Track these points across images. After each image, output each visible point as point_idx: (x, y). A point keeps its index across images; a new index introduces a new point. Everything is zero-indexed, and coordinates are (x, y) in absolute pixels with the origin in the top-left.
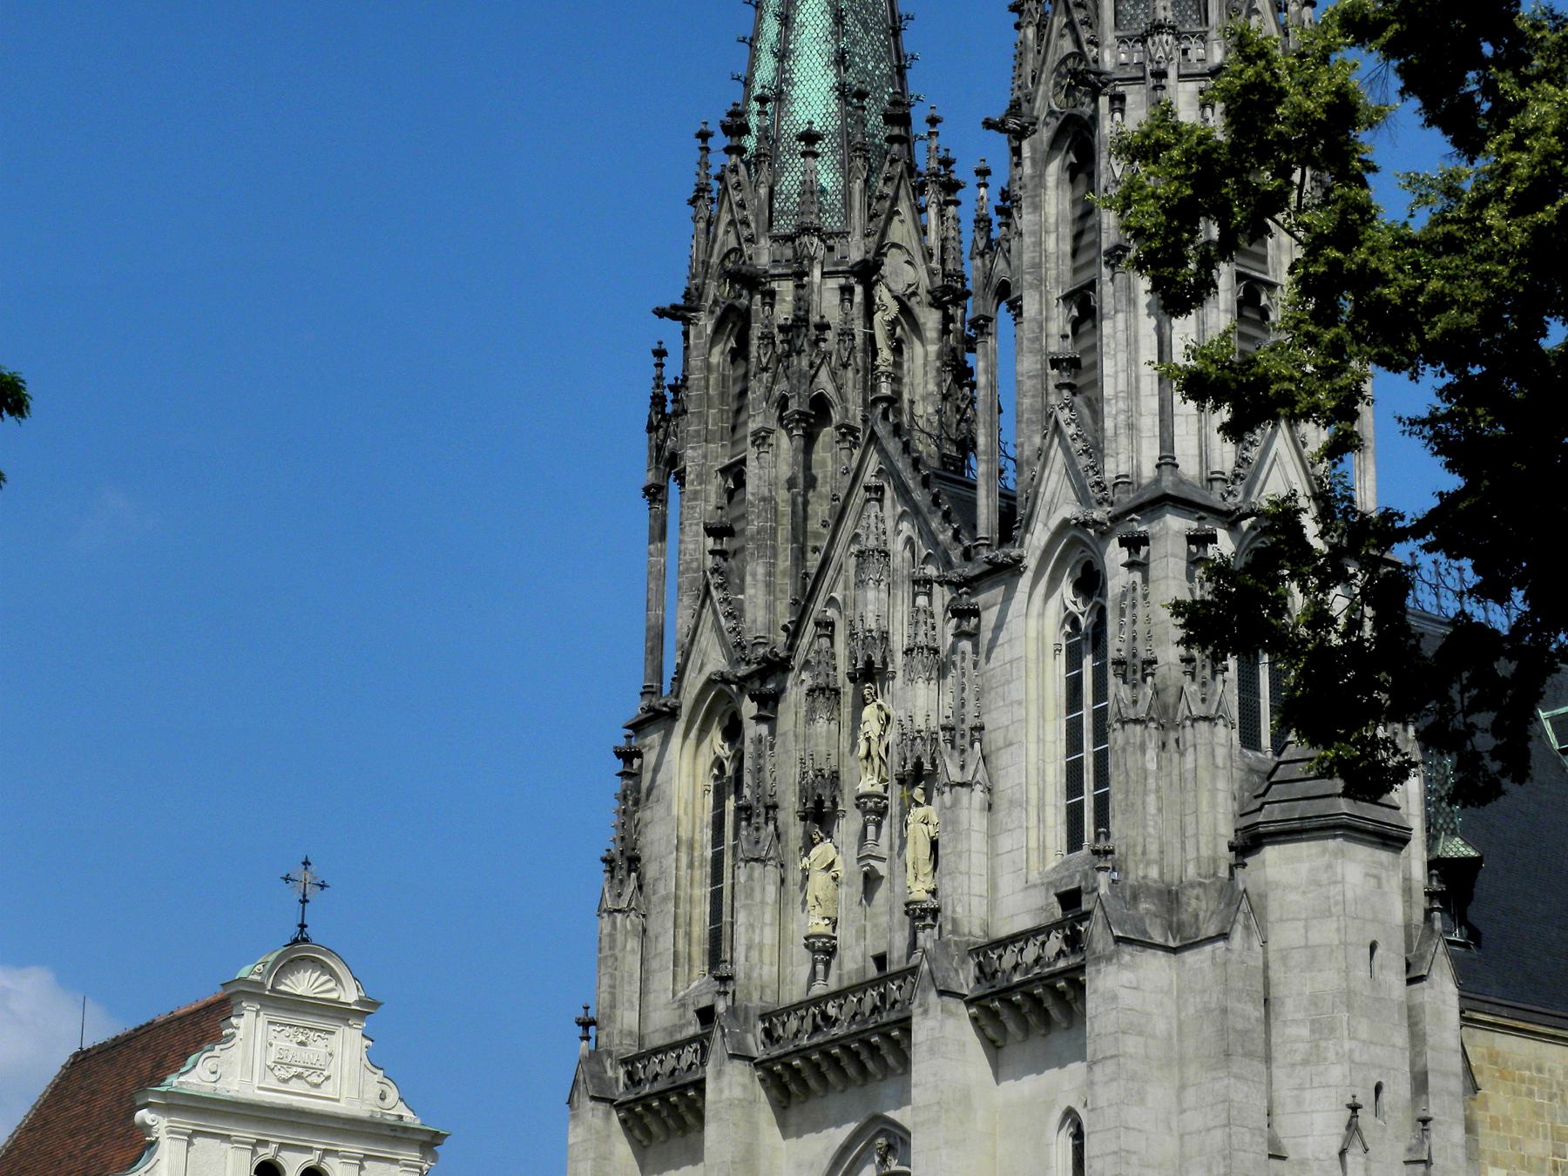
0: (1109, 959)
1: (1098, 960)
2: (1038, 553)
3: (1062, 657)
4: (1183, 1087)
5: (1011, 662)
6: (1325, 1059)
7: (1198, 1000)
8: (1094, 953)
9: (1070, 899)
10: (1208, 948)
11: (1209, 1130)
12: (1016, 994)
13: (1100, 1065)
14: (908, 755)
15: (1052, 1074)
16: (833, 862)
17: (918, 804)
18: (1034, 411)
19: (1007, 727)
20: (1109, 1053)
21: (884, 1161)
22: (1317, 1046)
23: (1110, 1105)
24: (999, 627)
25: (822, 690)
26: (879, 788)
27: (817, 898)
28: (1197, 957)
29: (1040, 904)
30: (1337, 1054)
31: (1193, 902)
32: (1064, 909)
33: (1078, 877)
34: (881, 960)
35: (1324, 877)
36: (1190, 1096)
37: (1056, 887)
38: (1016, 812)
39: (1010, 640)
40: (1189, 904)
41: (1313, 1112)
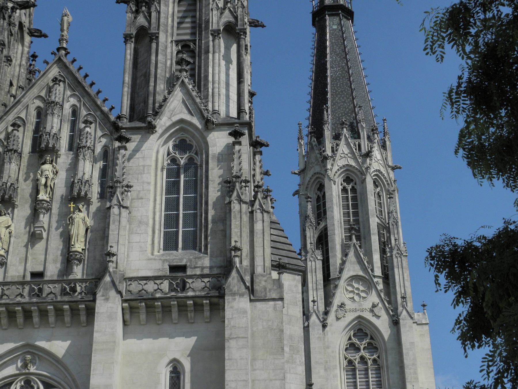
0: (242, 295)
1: (234, 294)
2: (164, 128)
3: (165, 172)
4: (254, 359)
5: (144, 166)
6: (295, 362)
7: (265, 324)
8: (231, 291)
9: (173, 269)
10: (272, 303)
11: (271, 380)
12: (158, 302)
13: (235, 340)
14: (83, 188)
15: (163, 341)
16: (10, 226)
17: (80, 211)
18: (162, 76)
19: (139, 191)
20: (241, 336)
21: (25, 366)
22: (292, 356)
23: (241, 359)
24: (136, 150)
25: (16, 151)
26: (48, 200)
28: (264, 306)
29: (158, 268)
30: (300, 361)
31: (263, 283)
32: (170, 272)
33: (185, 261)
34: (37, 275)
35: (294, 289)
36: (259, 364)
37: (169, 262)
39: (144, 157)
40: (260, 283)
41: (290, 383)
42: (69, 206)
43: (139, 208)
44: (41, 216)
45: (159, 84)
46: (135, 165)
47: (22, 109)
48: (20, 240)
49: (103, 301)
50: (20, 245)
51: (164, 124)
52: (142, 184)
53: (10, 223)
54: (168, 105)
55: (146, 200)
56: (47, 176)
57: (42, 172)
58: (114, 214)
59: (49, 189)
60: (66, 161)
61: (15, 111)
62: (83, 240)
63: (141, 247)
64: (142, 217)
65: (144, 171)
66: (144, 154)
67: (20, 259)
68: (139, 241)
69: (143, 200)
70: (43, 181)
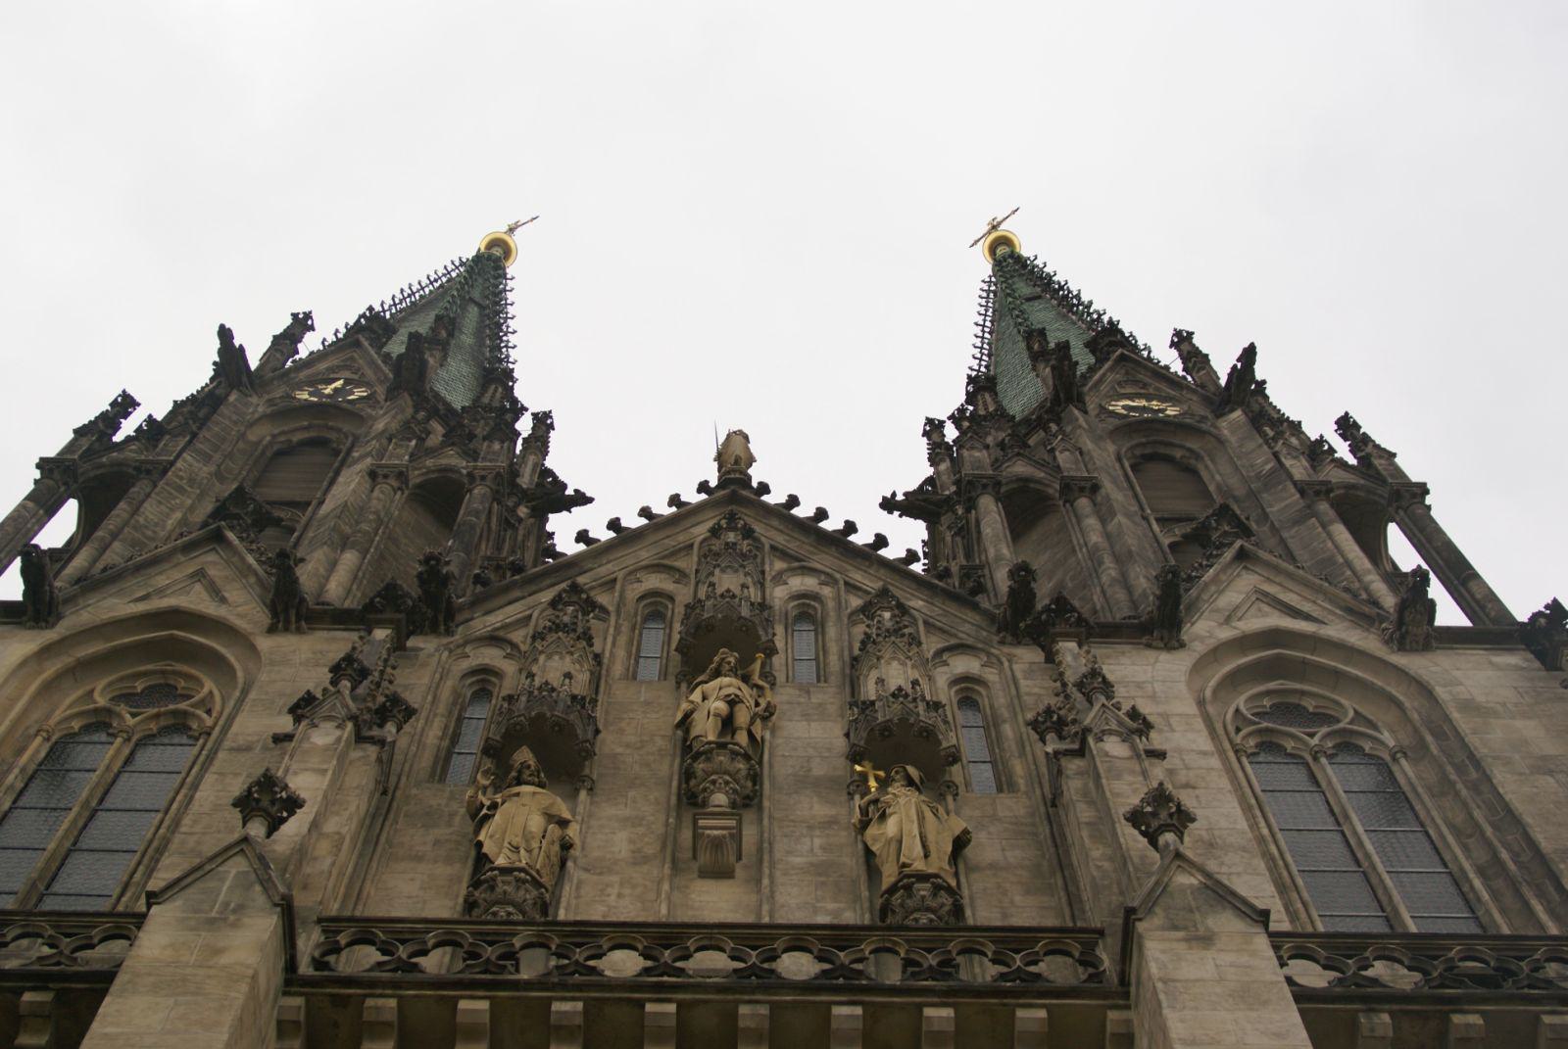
49: (1183, 946)
50: (614, 891)
69: (1197, 792)
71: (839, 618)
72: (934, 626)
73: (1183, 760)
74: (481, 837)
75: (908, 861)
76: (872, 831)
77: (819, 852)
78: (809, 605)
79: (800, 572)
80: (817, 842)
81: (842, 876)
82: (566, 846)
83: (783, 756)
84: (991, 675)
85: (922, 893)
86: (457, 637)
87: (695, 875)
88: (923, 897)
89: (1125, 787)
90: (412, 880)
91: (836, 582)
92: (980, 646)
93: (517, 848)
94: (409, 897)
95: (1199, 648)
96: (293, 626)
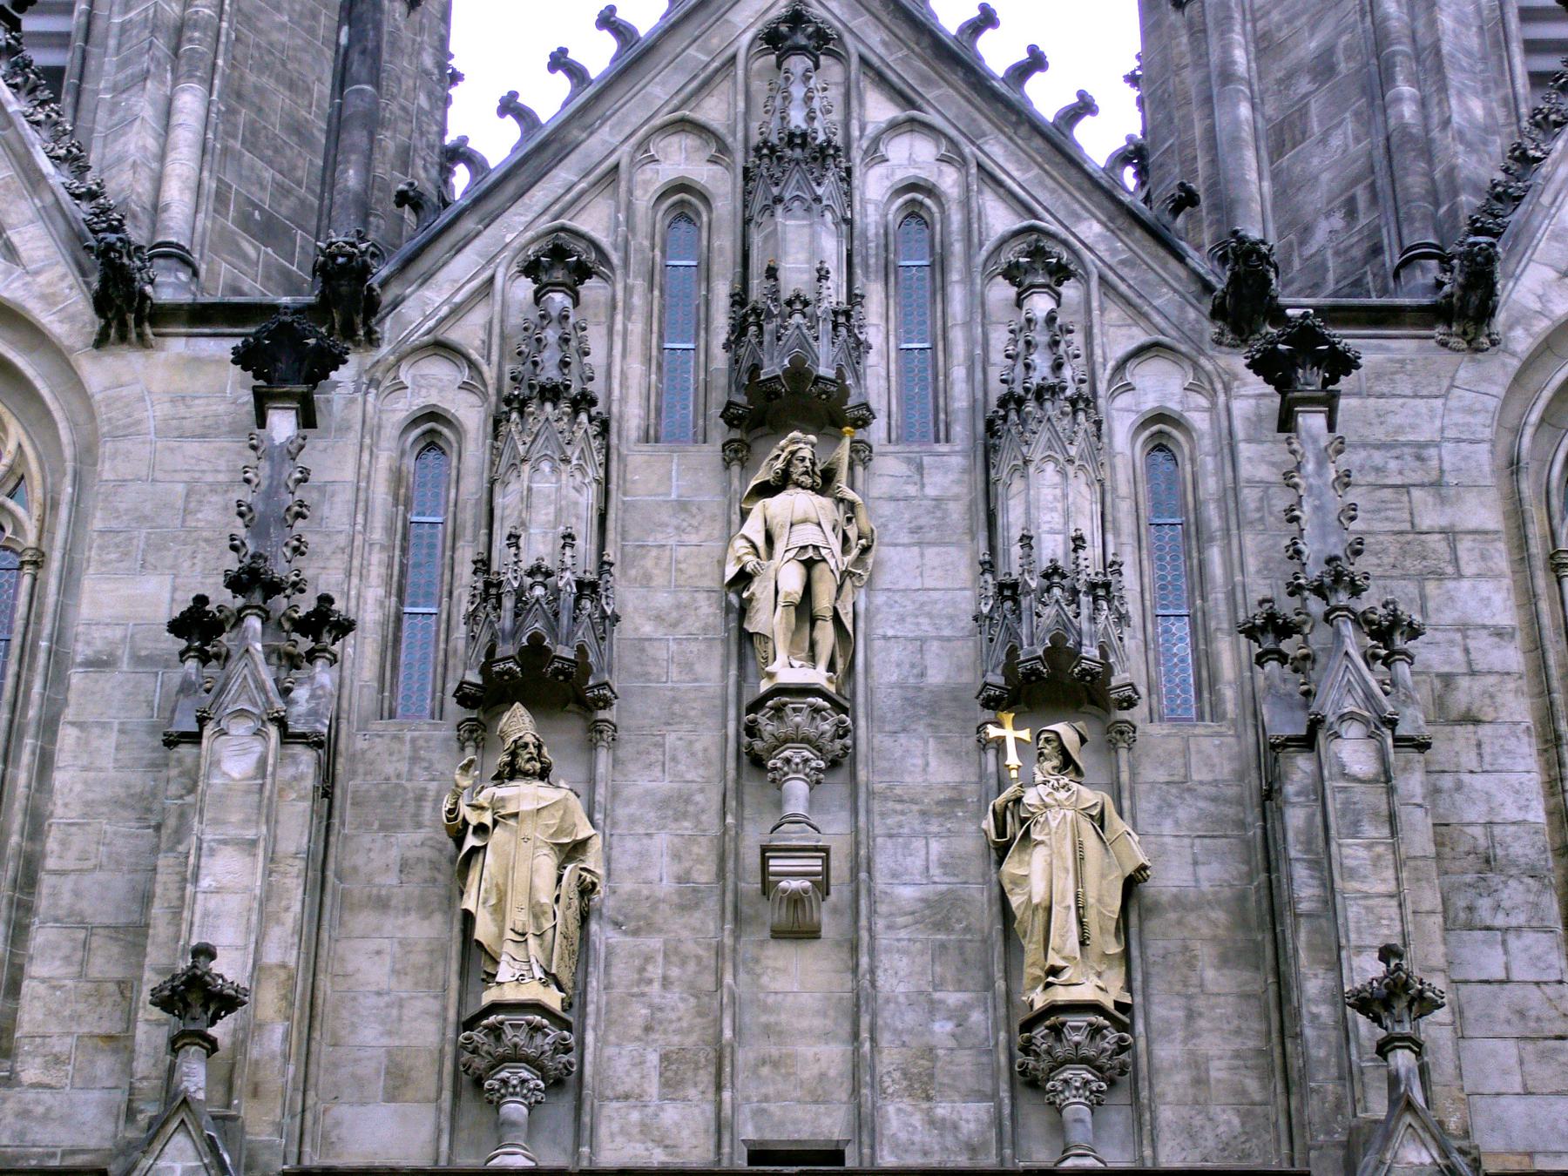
5: (1450, 534)
19: (1448, 679)
27: (537, 912)
38: (1514, 892)
39: (1437, 485)
42: (993, 731)
43: (1466, 778)
44: (797, 789)
45: (1460, 94)
46: (1388, 526)
47: (583, 185)
48: (655, 943)
50: (655, 971)
51: (1537, 306)
52: (1458, 637)
53: (585, 830)
54: (1546, 199)
55: (1504, 730)
56: (810, 553)
57: (770, 539)
58: (1345, 775)
59: (826, 635)
60: (912, 490)
61: (540, 195)
62: (1115, 949)
63: (1522, 1014)
64: (1497, 830)
65: (1456, 561)
66: (1434, 463)
67: (665, 1058)
68: (1502, 975)
69: (1485, 731)
70: (792, 580)
71: (969, 258)
72: (1114, 288)
73: (1467, 651)
74: (469, 903)
75: (1060, 963)
76: (1011, 867)
77: (935, 871)
78: (921, 204)
79: (907, 127)
80: (936, 847)
81: (967, 929)
82: (586, 891)
83: (885, 637)
84: (1200, 421)
85: (1077, 1038)
86: (385, 349)
87: (767, 933)
88: (1077, 1044)
89: (1362, 853)
90: (378, 953)
91: (964, 162)
92: (1183, 348)
93: (523, 935)
94: (379, 994)
95: (1522, 342)
96: (133, 336)
